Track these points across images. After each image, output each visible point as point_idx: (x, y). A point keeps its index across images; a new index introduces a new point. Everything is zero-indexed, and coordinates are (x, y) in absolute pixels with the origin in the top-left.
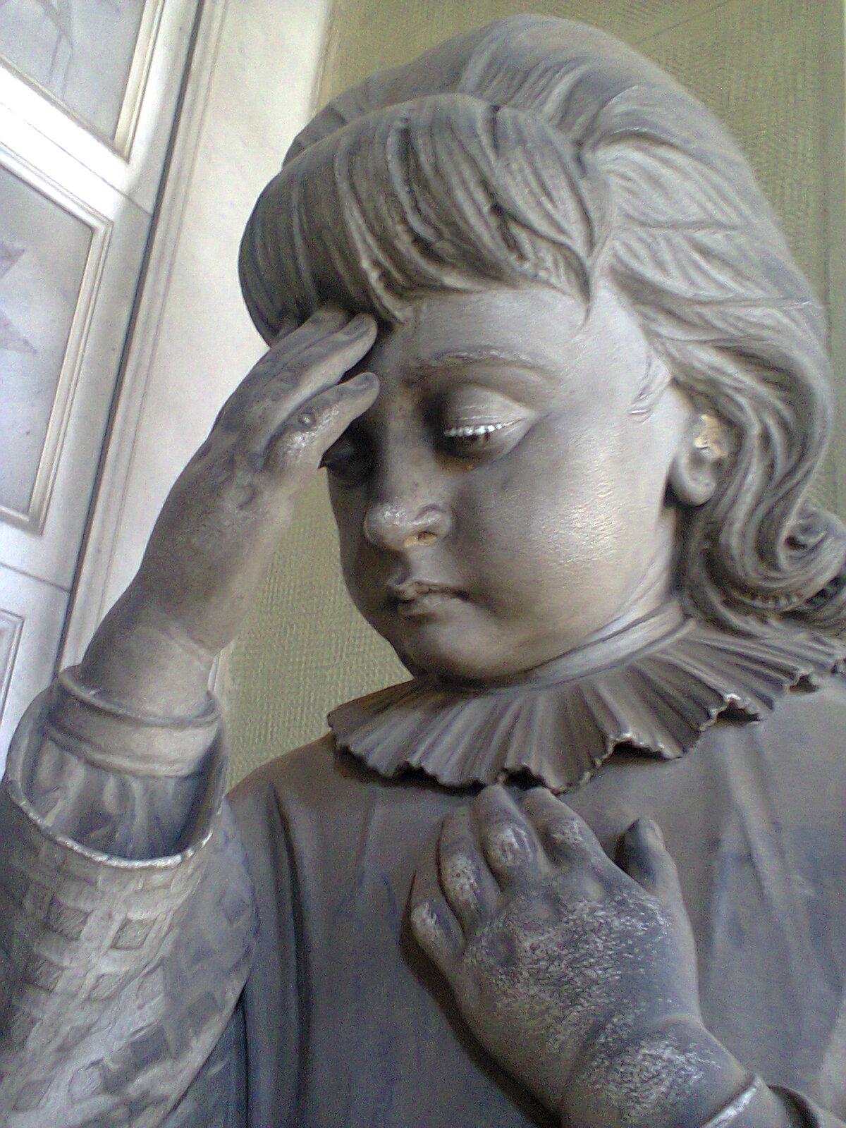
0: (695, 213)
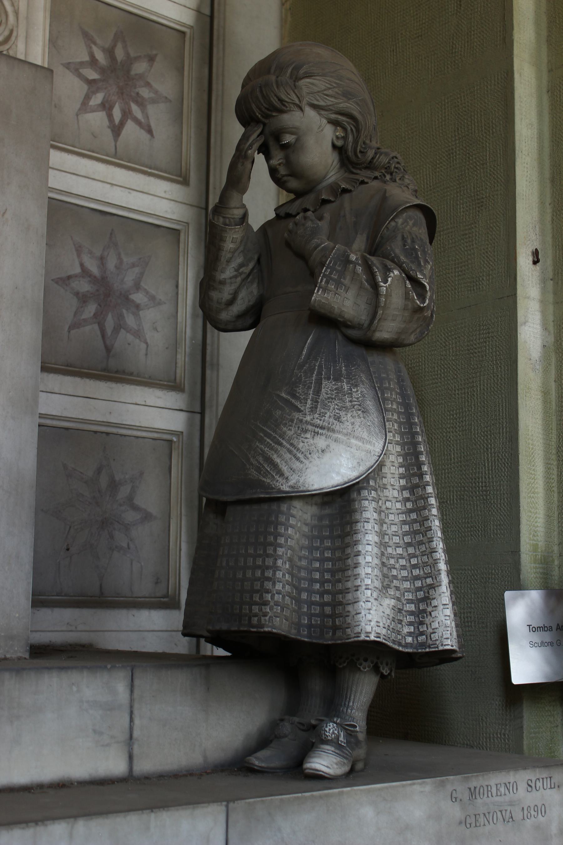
0: (323, 88)
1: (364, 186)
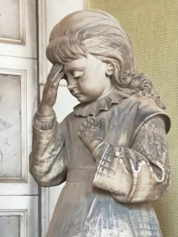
0: (98, 43)
1: (125, 100)
